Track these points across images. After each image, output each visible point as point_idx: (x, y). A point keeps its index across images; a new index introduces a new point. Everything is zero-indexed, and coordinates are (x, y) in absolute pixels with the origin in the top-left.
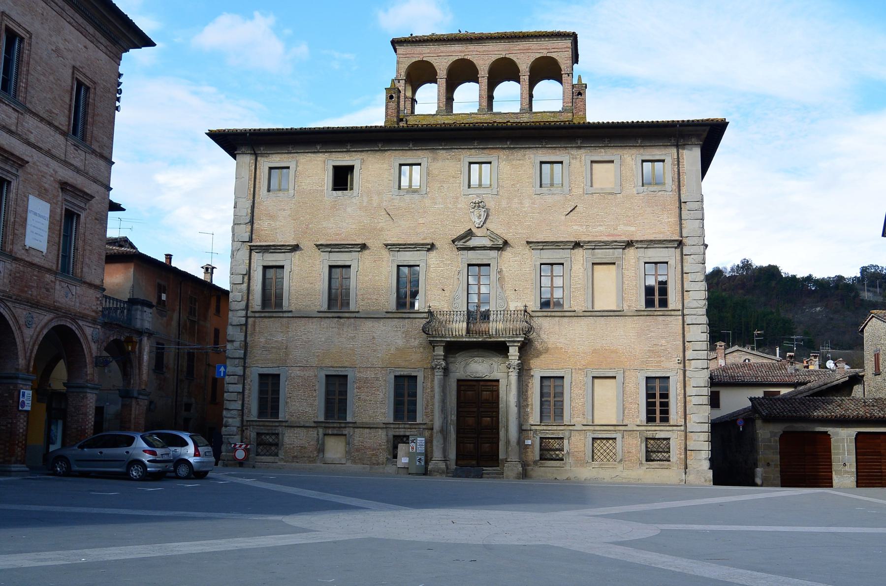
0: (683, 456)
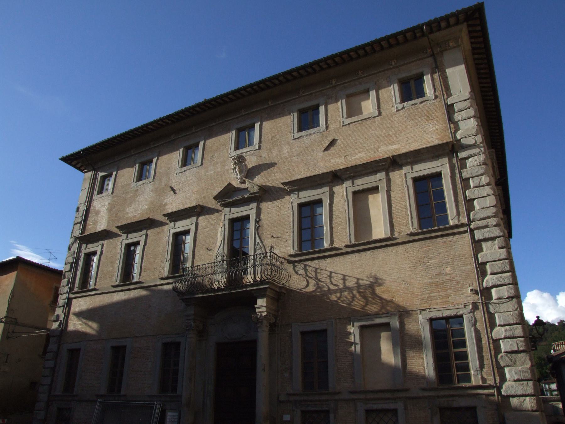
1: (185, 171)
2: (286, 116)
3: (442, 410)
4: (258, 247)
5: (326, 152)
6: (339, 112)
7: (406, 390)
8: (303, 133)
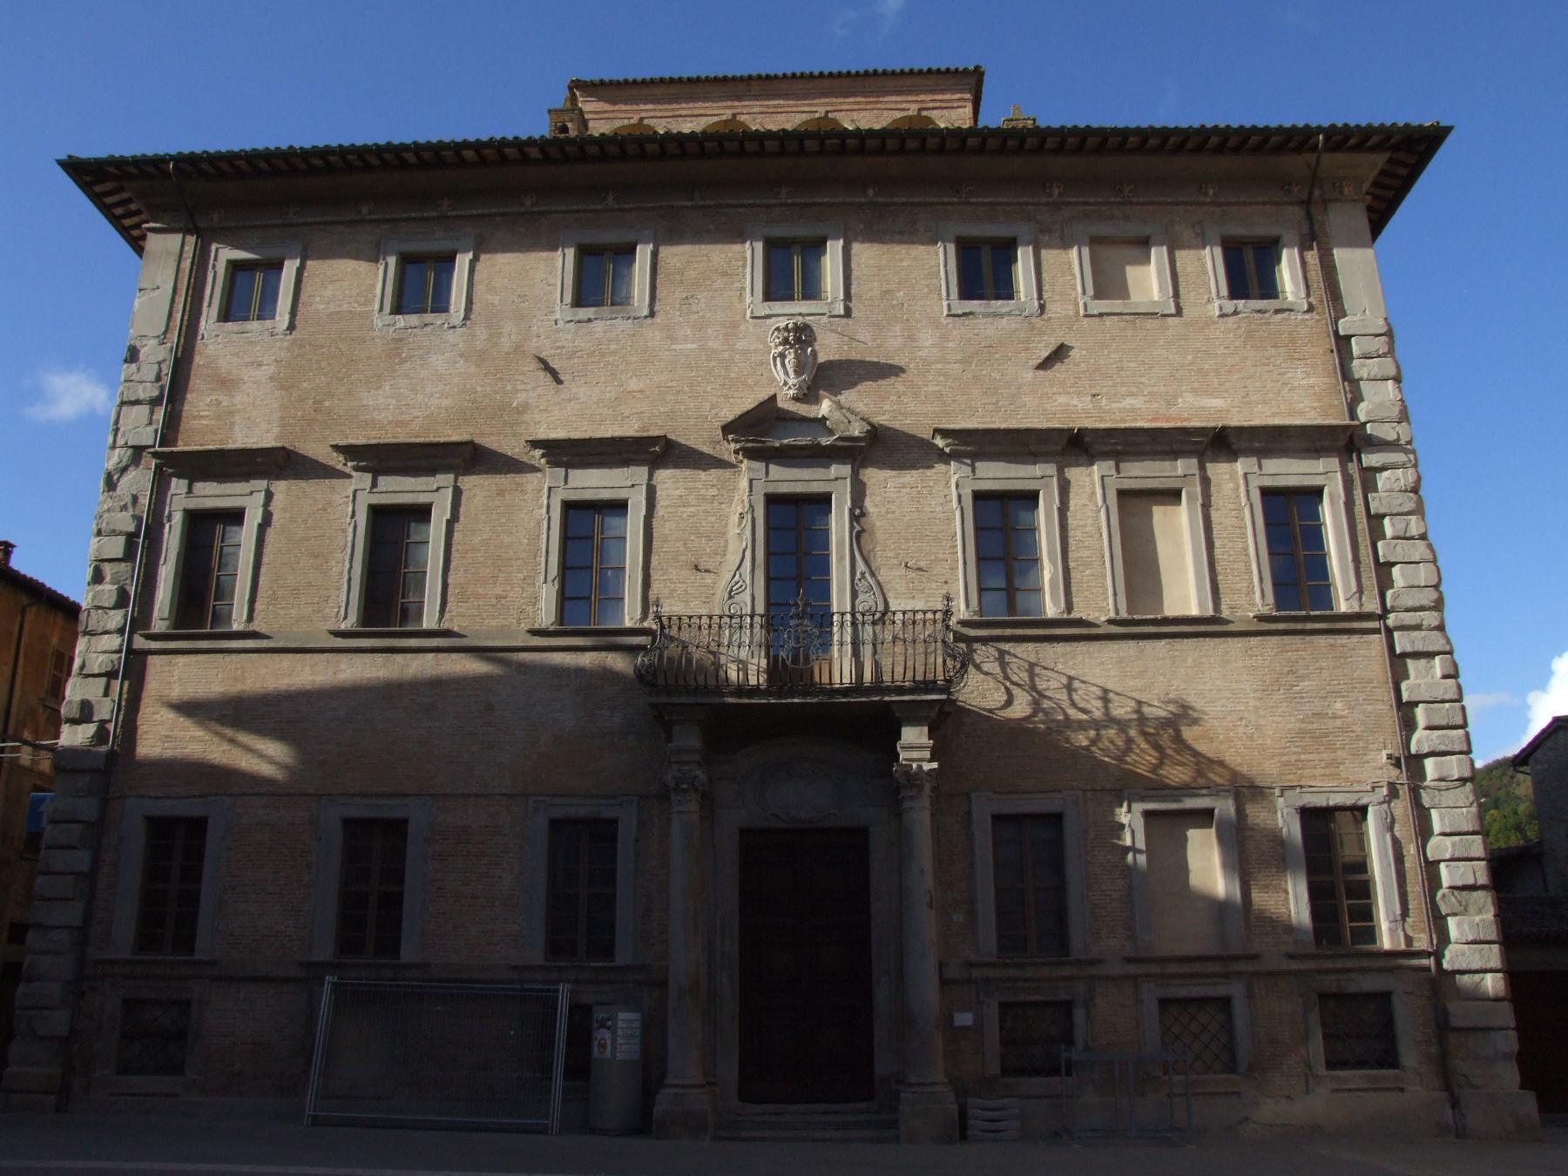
0: (1433, 1050)
1: (589, 320)
3: (1324, 997)
4: (861, 586)
5: (1041, 373)
7: (1254, 957)
8: (974, 305)
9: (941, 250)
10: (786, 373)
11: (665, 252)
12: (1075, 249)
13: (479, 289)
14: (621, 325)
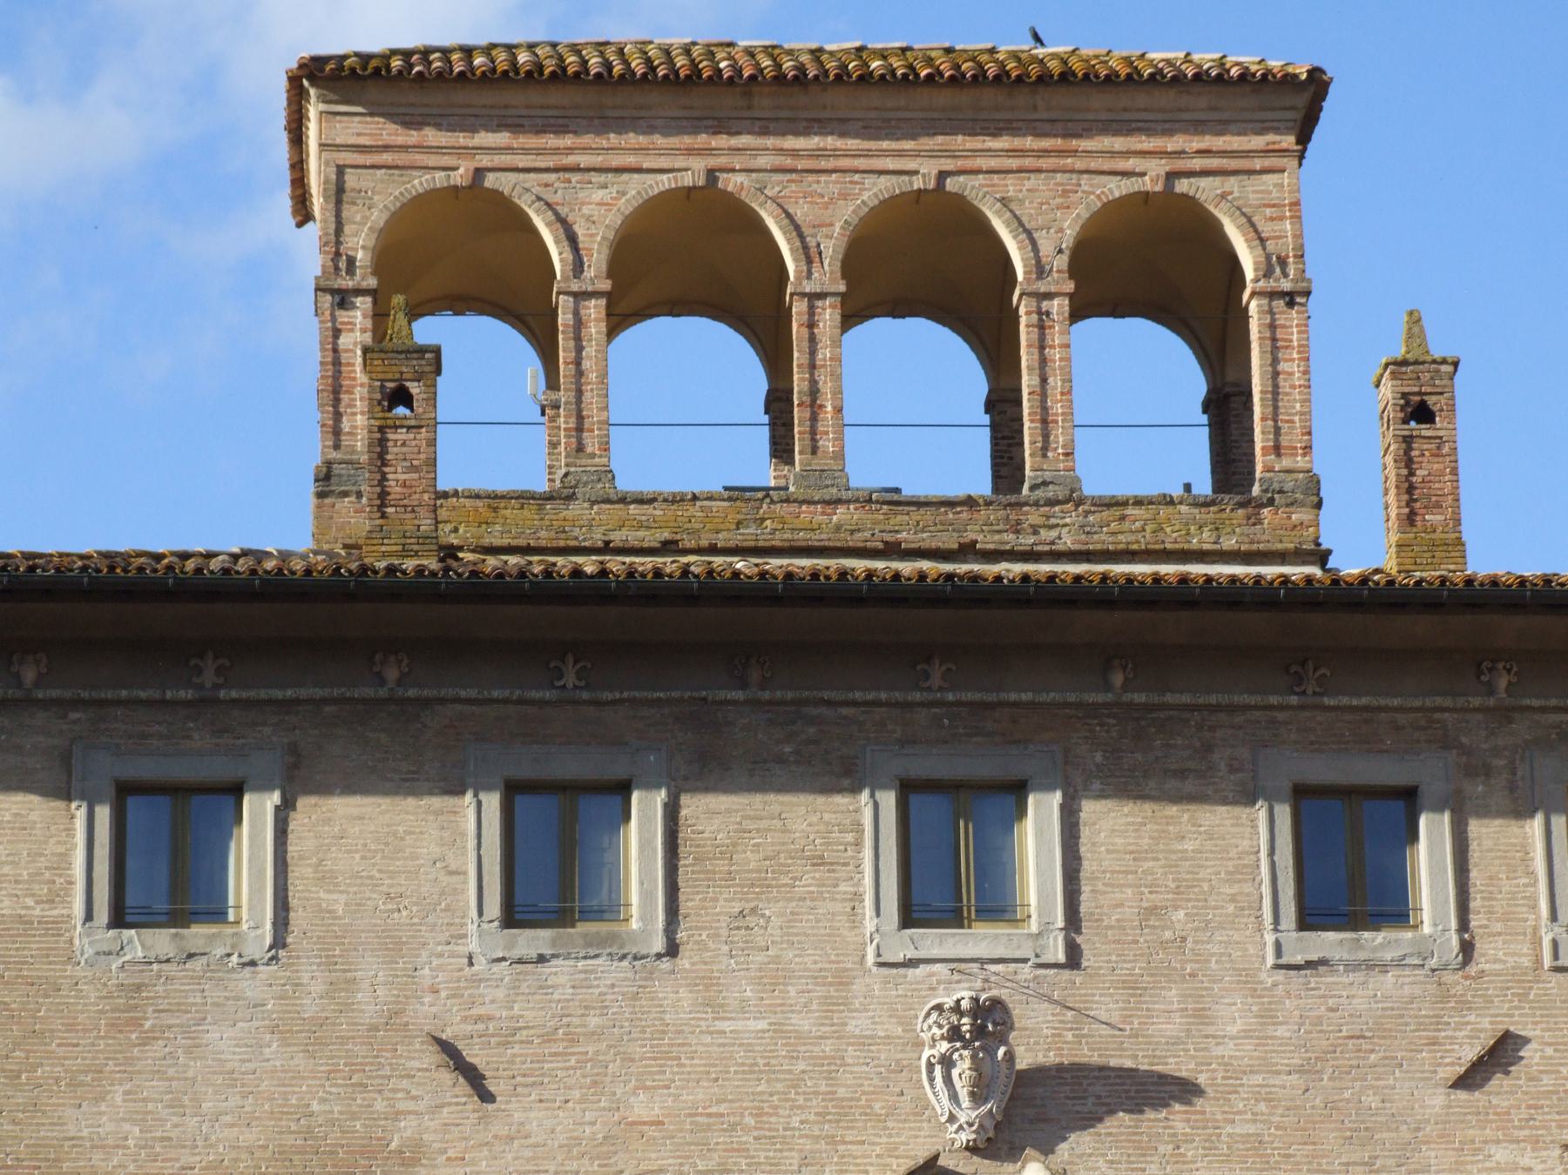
1: (541, 959)
2: (1225, 801)
5: (1462, 1095)
6: (1531, 873)
8: (1328, 942)
9: (1262, 815)
10: (954, 1097)
11: (692, 806)
12: (1538, 820)
13: (299, 875)
14: (610, 973)
